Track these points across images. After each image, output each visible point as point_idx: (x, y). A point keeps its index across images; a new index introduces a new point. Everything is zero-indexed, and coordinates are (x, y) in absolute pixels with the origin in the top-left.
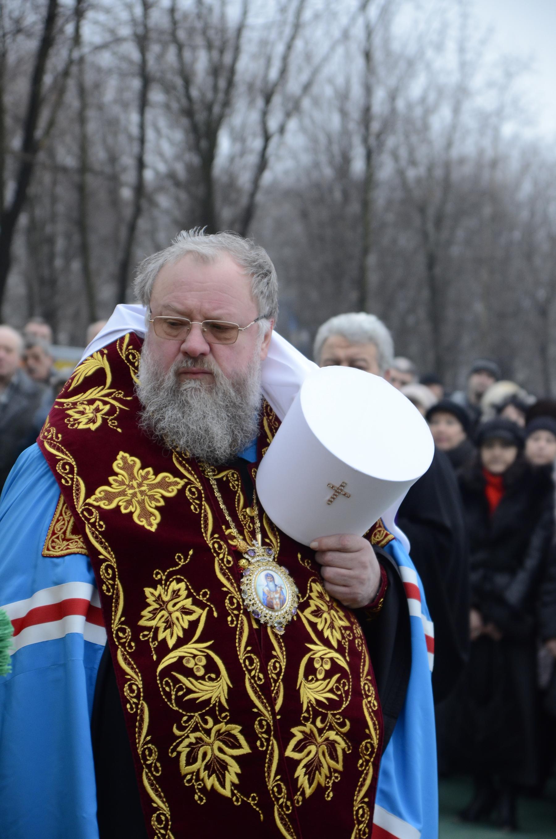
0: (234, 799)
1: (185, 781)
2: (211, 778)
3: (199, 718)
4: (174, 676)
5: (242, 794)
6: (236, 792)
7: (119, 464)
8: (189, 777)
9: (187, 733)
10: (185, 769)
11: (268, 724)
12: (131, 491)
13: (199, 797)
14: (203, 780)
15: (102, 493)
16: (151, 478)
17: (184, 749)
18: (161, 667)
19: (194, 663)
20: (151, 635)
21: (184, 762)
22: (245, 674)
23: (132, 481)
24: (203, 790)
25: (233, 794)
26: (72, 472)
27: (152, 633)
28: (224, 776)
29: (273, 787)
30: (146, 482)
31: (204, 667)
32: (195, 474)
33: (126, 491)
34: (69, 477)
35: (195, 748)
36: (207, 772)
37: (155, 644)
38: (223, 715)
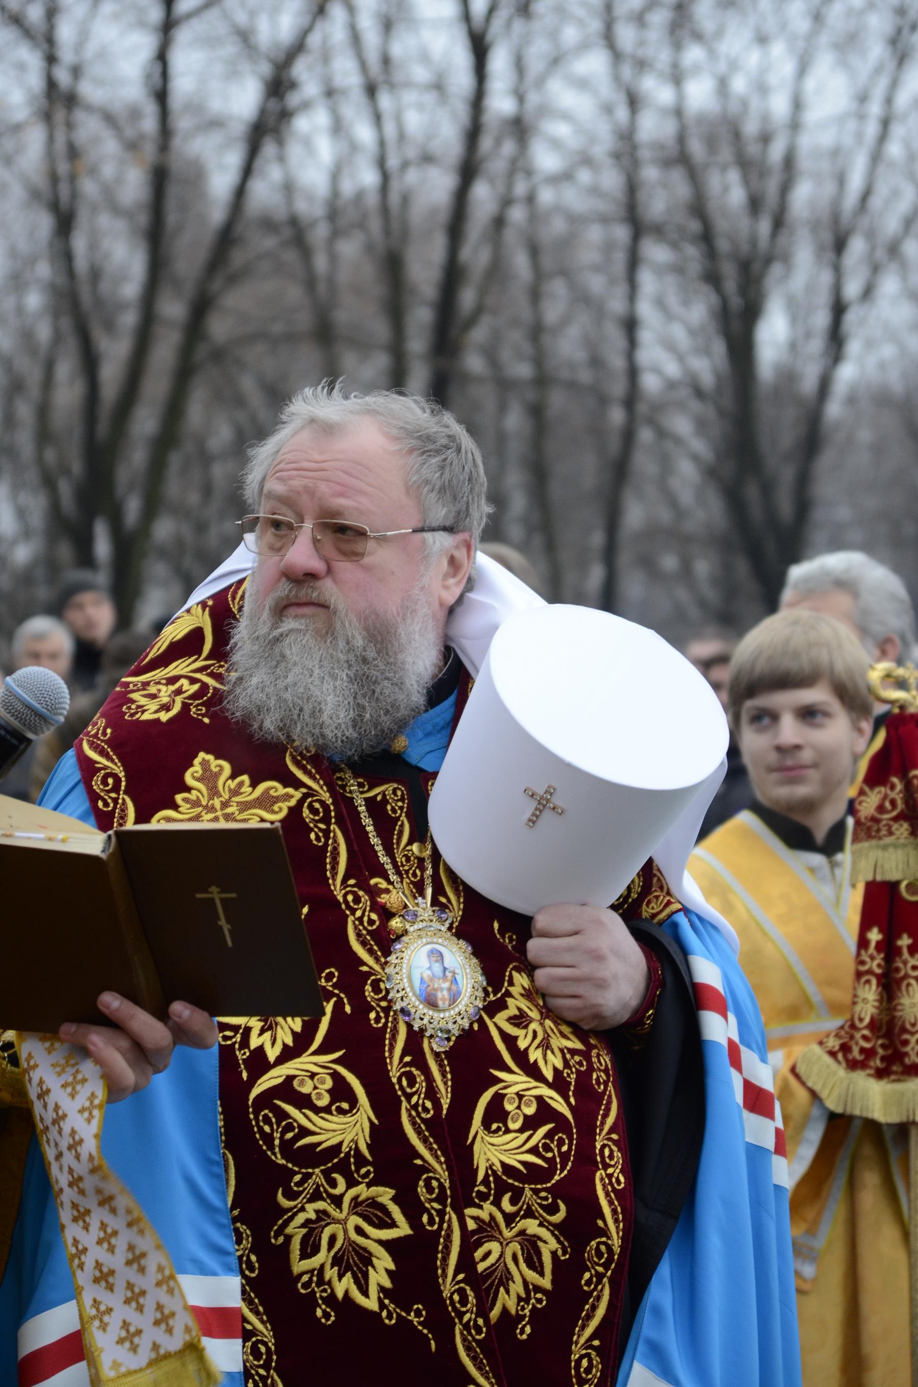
0: (384, 1314)
1: (300, 1285)
2: (344, 1280)
3: (322, 1177)
4: (279, 1107)
5: (397, 1305)
6: (387, 1301)
7: (196, 772)
8: (305, 1278)
9: (301, 1202)
10: (299, 1266)
11: (441, 1186)
13: (324, 1311)
14: (329, 1283)
17: (297, 1230)
18: (255, 1092)
19: (313, 1086)
20: (238, 1038)
21: (298, 1252)
22: (401, 1101)
24: (331, 1300)
25: (382, 1306)
26: (116, 788)
27: (239, 1036)
28: (366, 1276)
29: (452, 1294)
31: (328, 1091)
34: (110, 797)
35: (316, 1228)
36: (336, 1268)
37: (245, 1053)
38: (363, 1171)
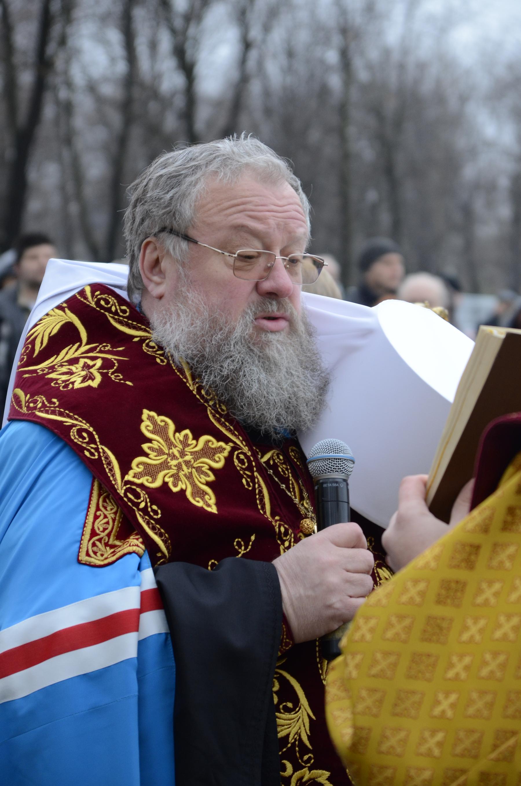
12: (174, 463)
15: (140, 466)
16: (192, 444)
23: (171, 449)
30: (186, 449)
32: (240, 434)
33: (168, 462)
